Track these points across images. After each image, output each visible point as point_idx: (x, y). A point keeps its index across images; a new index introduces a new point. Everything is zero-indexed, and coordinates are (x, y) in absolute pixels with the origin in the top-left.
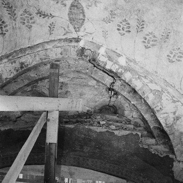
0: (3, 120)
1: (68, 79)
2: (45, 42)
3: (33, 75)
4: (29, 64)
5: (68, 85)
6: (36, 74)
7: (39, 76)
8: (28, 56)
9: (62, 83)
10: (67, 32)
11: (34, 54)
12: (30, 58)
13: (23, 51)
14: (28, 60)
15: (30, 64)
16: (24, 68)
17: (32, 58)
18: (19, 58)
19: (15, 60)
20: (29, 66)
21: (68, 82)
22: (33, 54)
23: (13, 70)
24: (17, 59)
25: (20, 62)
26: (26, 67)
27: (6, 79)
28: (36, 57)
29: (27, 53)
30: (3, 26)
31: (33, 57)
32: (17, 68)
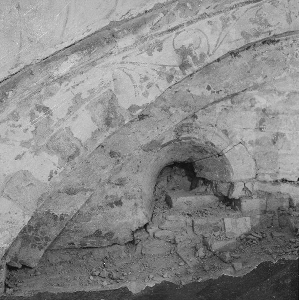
0: (89, 244)
1: (280, 98)
3: (197, 92)
4: (206, 52)
5: (280, 116)
6: (209, 88)
7: (218, 92)
8: (203, 22)
9: (264, 111)
11: (221, 18)
12: (207, 29)
13: (188, 5)
14: (204, 40)
15: (211, 53)
16: (190, 66)
17: (218, 33)
18: (174, 32)
19: (161, 39)
20: (208, 60)
21: (280, 108)
22: (218, 17)
23: (154, 77)
24: (166, 36)
25: (178, 46)
26: (196, 63)
27: (132, 108)
28: (227, 26)
29: (201, 12)
31: (219, 24)
32: (168, 68)
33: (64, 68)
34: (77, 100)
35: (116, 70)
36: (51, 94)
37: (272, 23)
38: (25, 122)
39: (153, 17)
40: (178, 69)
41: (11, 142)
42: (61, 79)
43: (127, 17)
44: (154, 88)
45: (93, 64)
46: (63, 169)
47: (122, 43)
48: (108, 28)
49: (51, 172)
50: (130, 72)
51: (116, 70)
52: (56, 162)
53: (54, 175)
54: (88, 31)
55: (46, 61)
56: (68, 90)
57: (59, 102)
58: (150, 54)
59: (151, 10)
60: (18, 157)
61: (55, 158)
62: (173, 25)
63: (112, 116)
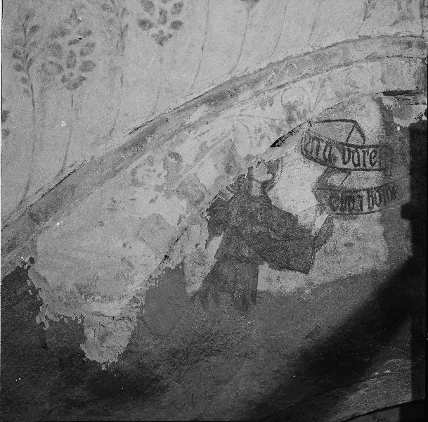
2: (347, 41)
8: (304, 82)
10: (404, 18)
13: (294, 65)
18: (282, 89)
19: (272, 94)
23: (266, 130)
26: (300, 118)
27: (249, 158)
32: (277, 122)
33: (196, 115)
34: (204, 148)
35: (236, 122)
36: (182, 142)
37: (359, 86)
38: (159, 168)
39: (267, 75)
40: (285, 123)
41: (146, 186)
42: (192, 127)
43: (245, 73)
44: (266, 139)
45: (217, 115)
46: (190, 213)
47: (241, 97)
48: (231, 81)
49: (180, 217)
50: (246, 124)
51: (236, 122)
52: (185, 206)
53: (183, 219)
54: (213, 84)
55: (179, 111)
56: (196, 138)
57: (188, 148)
58: (263, 109)
59: (265, 68)
60: (152, 201)
61: (184, 203)
62: (282, 83)
63: (231, 164)
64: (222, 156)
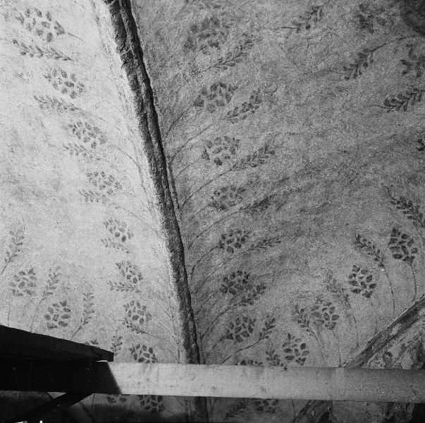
30: (405, 244)
38: (381, 360)
42: (394, 337)
45: (410, 326)
54: (405, 309)
64: (414, 351)
